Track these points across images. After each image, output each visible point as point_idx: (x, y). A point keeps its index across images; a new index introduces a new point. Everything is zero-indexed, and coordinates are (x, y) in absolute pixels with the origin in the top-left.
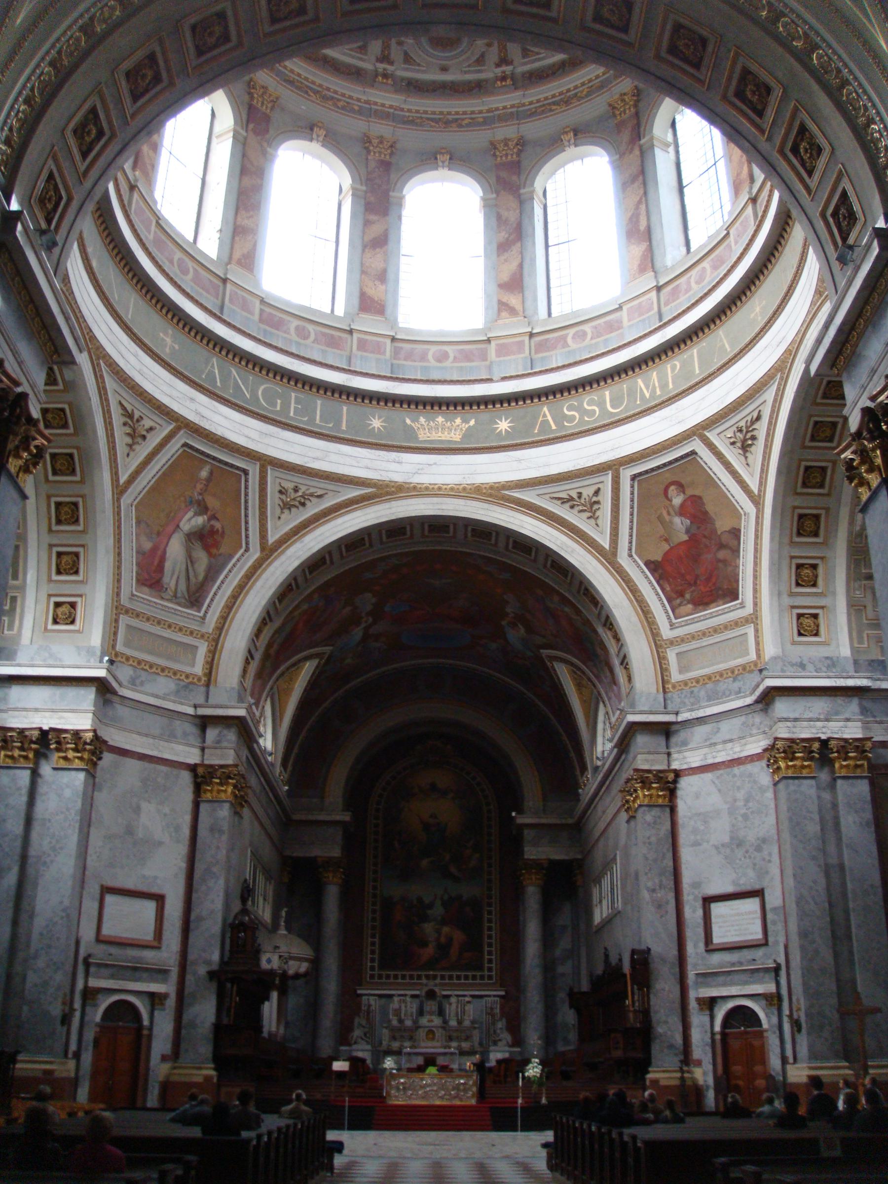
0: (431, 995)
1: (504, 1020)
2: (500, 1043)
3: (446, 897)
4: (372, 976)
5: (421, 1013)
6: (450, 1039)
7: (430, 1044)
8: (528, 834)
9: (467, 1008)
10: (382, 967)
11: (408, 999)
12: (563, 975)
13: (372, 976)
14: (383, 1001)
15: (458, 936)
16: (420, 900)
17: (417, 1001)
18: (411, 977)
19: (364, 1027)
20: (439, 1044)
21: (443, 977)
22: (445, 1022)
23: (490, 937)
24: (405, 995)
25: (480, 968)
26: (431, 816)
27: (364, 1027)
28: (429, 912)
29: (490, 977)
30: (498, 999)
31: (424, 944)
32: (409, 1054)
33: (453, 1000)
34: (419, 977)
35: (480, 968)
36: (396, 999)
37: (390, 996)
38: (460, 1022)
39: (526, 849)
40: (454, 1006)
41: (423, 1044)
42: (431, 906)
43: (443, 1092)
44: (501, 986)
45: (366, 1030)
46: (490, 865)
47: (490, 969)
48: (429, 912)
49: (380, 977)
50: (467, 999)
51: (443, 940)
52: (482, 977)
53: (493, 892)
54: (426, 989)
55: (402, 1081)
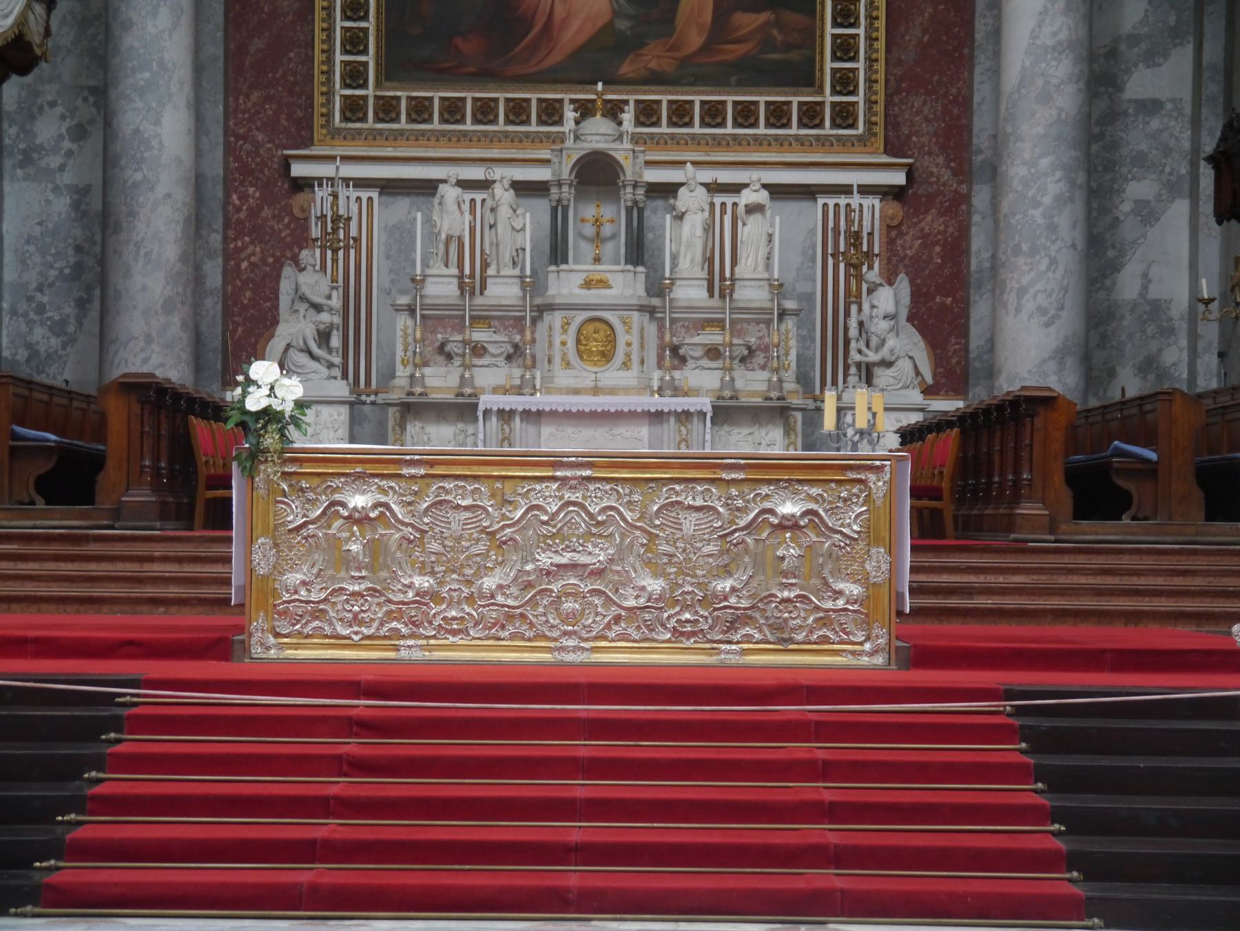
1: (903, 284)
2: (883, 377)
4: (354, 109)
5: (558, 253)
6: (676, 356)
7: (584, 375)
9: (745, 232)
10: (391, 71)
11: (503, 195)
12: (1151, 107)
13: (354, 109)
14: (402, 205)
17: (542, 207)
18: (518, 112)
19: (318, 308)
20: (629, 378)
21: (647, 114)
22: (658, 288)
24: (485, 185)
25: (806, 77)
27: (318, 308)
30: (876, 201)
32: (506, 415)
33: (692, 200)
34: (551, 112)
35: (806, 77)
36: (450, 193)
37: (428, 188)
40: (693, 226)
41: (563, 378)
43: (655, 585)
45: (325, 317)
47: (844, 82)
49: (387, 109)
50: (747, 197)
52: (811, 115)
54: (574, 152)
55: (359, 501)
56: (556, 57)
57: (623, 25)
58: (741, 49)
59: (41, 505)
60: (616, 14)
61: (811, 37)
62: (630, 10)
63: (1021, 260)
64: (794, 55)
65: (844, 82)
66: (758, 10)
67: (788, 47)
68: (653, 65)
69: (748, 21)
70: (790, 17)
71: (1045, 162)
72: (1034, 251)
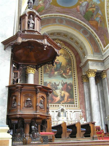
0: (62, 110)
1: (84, 118)
3: (62, 83)
8: (90, 63)
11: (55, 112)
15: (67, 94)
16: (55, 83)
23: (76, 94)
24: (53, 111)
25: (73, 103)
26: (57, 60)
28: (57, 87)
29: (77, 106)
31: (57, 96)
38: (71, 119)
39: (90, 67)
42: (58, 85)
44: (80, 109)
46: (74, 74)
48: (57, 87)
51: (62, 95)
52: (74, 106)
53: (76, 82)
54: (61, 109)
56: (56, 102)
57: (61, 100)
58: (69, 101)
59: (84, 137)
60: (60, 99)
61: (74, 101)
62: (61, 98)
63: (95, 116)
64: (73, 102)
65: (76, 104)
66: (70, 99)
67: (72, 101)
68: (63, 102)
69: (69, 99)
70: (72, 99)
71: (96, 109)
72: (96, 115)
